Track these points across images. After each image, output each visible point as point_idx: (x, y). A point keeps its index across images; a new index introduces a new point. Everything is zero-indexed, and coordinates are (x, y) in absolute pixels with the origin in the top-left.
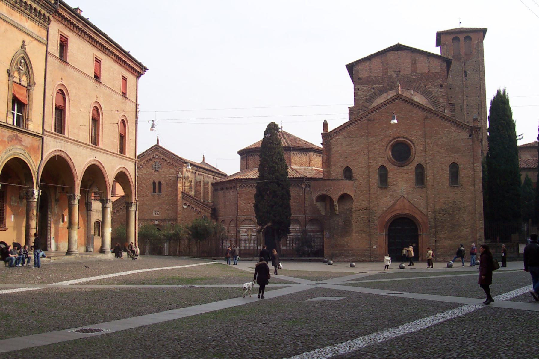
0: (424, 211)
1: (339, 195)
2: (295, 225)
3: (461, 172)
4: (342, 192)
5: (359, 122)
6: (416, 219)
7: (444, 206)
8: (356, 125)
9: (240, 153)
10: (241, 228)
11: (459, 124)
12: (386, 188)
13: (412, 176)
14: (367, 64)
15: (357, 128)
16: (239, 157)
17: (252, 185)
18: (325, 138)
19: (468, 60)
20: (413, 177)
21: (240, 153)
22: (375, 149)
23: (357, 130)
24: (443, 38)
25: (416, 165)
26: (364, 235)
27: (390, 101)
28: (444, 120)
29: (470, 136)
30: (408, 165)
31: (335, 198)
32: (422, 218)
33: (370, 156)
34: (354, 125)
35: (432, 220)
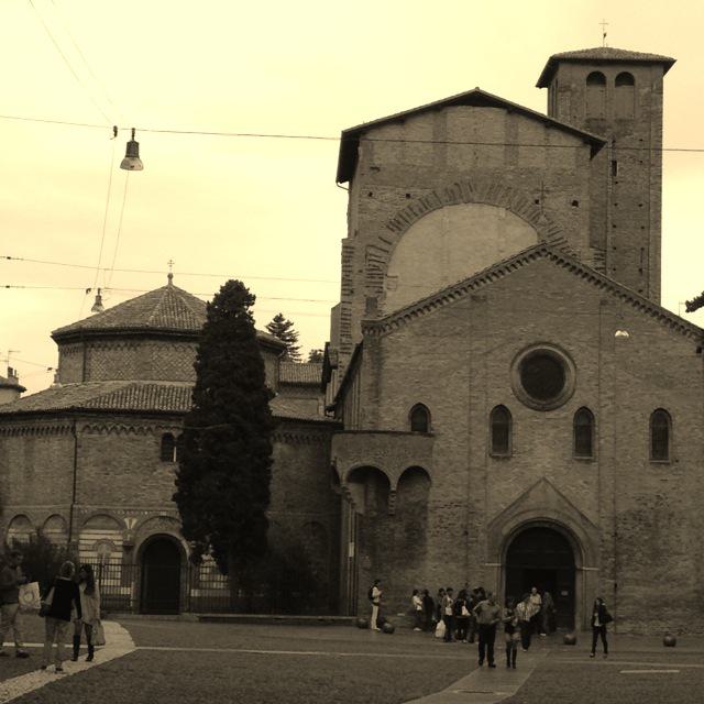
0: (590, 514)
1: (403, 468)
3: (675, 432)
4: (411, 463)
5: (451, 300)
6: (571, 532)
7: (636, 507)
8: (444, 307)
9: (62, 337)
10: (82, 536)
11: (676, 323)
12: (508, 458)
13: (566, 435)
14: (394, 132)
15: (444, 316)
16: (56, 346)
17: (118, 427)
18: (371, 332)
19: (624, 135)
20: (568, 435)
21: (62, 337)
22: (486, 366)
23: (447, 318)
24: (563, 73)
25: (576, 409)
26: (453, 566)
27: (525, 259)
28: (643, 311)
29: (699, 351)
30: (558, 407)
31: (394, 478)
32: (586, 533)
33: (475, 383)
34: (439, 305)
35: (607, 537)
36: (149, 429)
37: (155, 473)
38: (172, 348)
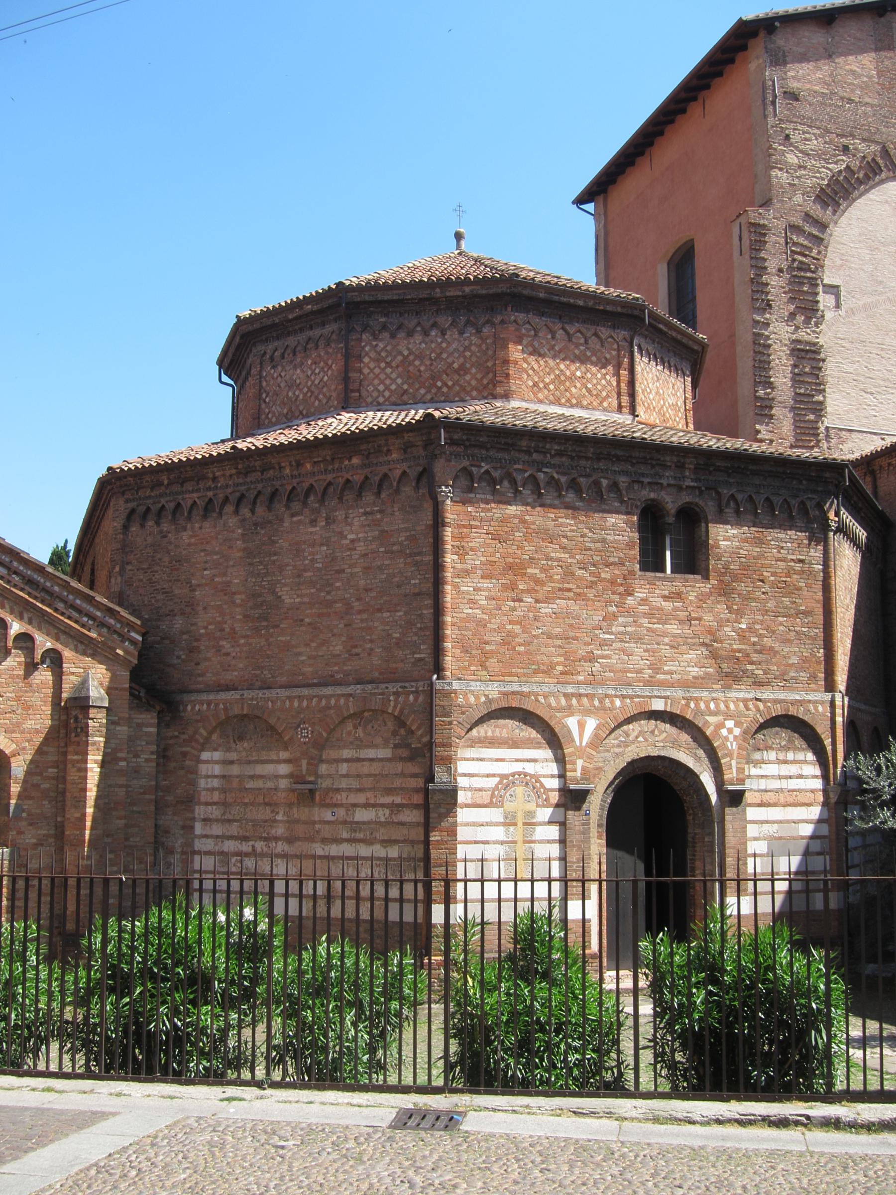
2: (790, 756)
10: (462, 767)
17: (541, 476)
36: (614, 487)
37: (630, 601)
38: (560, 333)
